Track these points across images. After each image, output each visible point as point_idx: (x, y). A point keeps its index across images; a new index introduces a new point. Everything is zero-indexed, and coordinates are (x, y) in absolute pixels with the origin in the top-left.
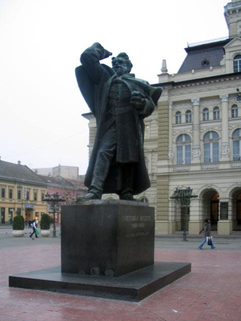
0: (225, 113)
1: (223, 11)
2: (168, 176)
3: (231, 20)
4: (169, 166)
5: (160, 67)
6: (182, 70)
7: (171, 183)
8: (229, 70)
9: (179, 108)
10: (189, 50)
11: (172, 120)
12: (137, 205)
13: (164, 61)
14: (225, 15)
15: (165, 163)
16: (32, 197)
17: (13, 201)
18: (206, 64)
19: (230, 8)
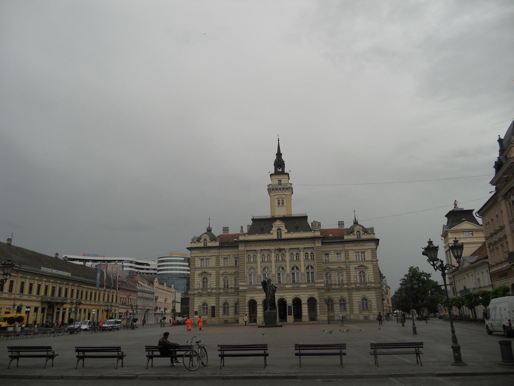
0: (273, 259)
1: (267, 188)
2: (245, 291)
3: (272, 194)
4: (245, 286)
5: (240, 230)
6: (252, 231)
7: (247, 295)
8: (275, 236)
9: (249, 253)
10: (253, 220)
11: (246, 260)
12: (233, 309)
13: (242, 227)
14: (268, 190)
15: (244, 284)
16: (110, 300)
17: (100, 304)
18: (262, 231)
19: (271, 187)
